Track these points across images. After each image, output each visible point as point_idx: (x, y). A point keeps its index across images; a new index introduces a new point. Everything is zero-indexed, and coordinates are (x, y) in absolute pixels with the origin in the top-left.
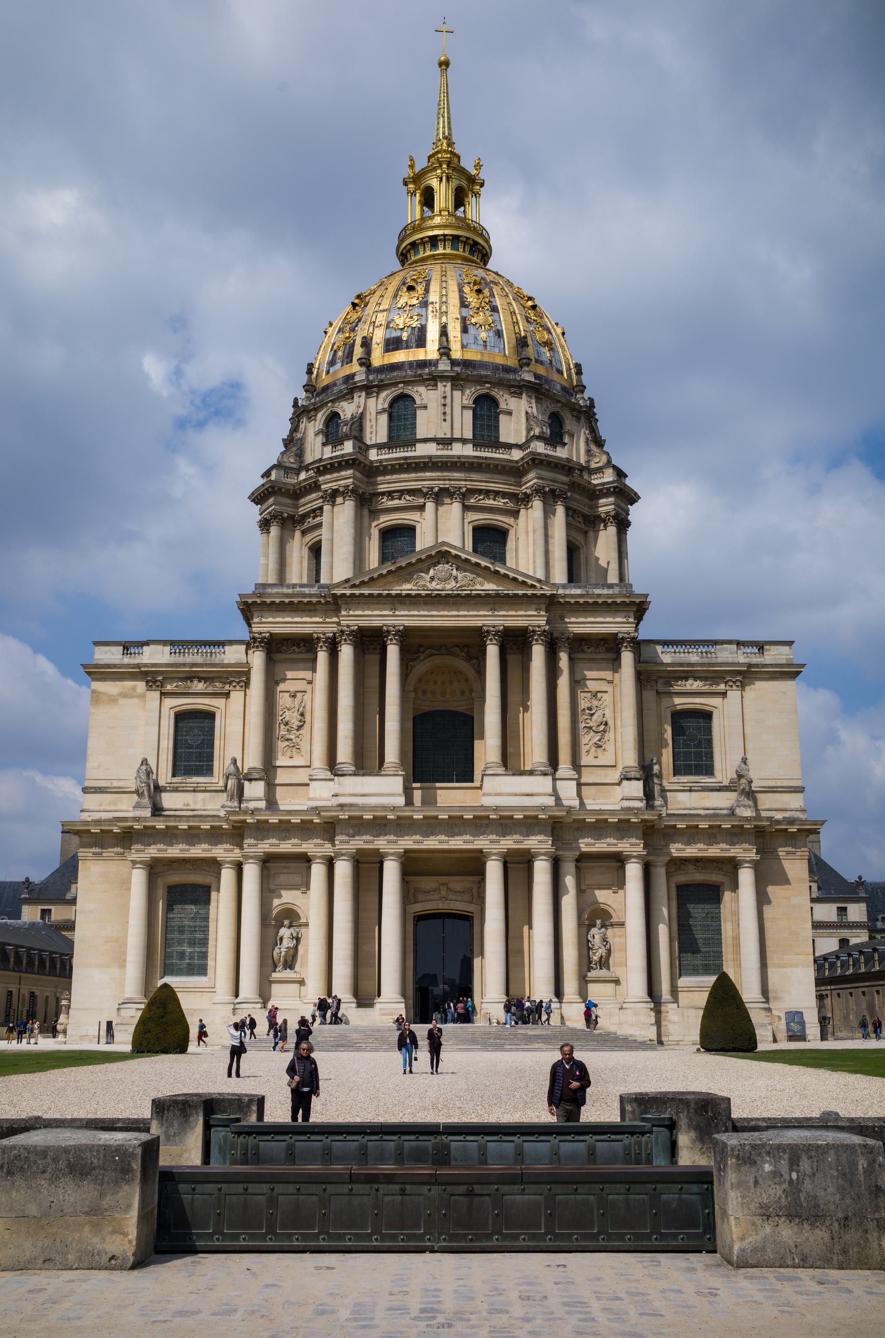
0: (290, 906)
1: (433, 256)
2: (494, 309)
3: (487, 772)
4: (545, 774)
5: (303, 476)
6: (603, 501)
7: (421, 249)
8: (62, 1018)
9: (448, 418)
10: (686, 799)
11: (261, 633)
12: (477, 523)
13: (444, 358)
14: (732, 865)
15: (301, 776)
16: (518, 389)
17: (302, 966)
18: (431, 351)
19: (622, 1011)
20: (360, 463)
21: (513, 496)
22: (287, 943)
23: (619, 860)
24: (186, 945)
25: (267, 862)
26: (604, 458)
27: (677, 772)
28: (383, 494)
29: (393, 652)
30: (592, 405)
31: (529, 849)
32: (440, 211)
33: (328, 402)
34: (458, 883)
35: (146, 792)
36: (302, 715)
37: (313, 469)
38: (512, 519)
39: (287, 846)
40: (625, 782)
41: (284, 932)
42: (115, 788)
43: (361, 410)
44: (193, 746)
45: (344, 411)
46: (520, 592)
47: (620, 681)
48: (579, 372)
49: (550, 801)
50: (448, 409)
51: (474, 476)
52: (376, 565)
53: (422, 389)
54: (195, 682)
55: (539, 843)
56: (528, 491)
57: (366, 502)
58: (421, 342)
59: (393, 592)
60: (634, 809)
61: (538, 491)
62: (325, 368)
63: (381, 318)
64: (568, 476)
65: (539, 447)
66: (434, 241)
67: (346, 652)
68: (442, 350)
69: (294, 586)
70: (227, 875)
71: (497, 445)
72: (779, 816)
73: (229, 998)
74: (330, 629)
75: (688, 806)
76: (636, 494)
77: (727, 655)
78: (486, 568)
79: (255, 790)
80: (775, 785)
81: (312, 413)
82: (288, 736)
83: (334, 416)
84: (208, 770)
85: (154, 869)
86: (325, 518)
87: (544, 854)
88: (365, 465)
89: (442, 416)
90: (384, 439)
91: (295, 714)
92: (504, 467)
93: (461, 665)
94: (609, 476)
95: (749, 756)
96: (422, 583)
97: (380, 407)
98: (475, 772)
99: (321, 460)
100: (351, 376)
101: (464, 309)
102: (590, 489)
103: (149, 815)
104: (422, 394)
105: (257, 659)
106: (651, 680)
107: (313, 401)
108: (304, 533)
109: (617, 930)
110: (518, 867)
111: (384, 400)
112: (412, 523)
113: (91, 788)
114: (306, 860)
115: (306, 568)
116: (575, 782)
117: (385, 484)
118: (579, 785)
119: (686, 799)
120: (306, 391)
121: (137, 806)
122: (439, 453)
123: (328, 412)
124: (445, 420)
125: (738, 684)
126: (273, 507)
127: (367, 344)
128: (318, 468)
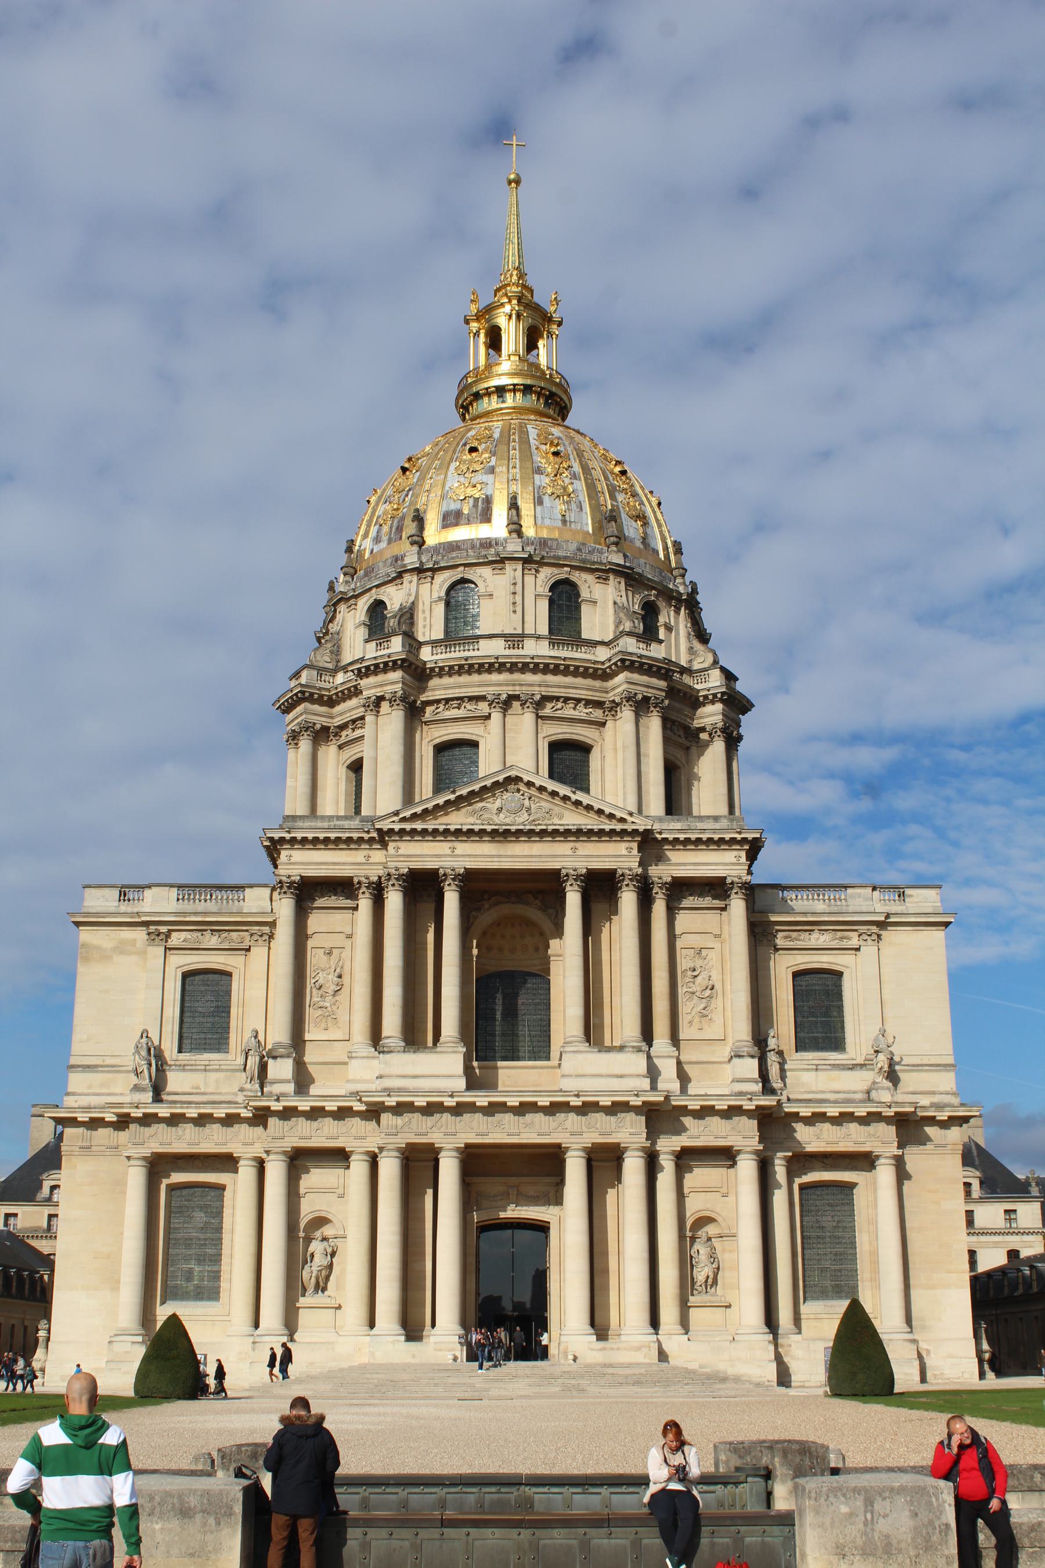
0: (323, 1214)
1: (501, 409)
2: (574, 476)
3: (567, 1049)
4: (639, 1050)
5: (340, 678)
6: (709, 709)
7: (486, 400)
8: (40, 1353)
9: (519, 609)
10: (811, 1080)
11: (289, 877)
12: (554, 738)
13: (514, 535)
16: (602, 573)
17: (337, 1289)
18: (497, 528)
19: (733, 1344)
20: (411, 664)
21: (598, 704)
22: (320, 1261)
23: (726, 1156)
24: (193, 1262)
26: (710, 659)
27: (801, 1045)
28: (438, 701)
29: (451, 900)
30: (695, 591)
31: (619, 1144)
32: (509, 356)
33: (370, 589)
35: (146, 1072)
36: (340, 977)
37: (352, 671)
38: (597, 733)
40: (735, 1060)
41: (316, 1247)
42: (108, 1066)
43: (412, 599)
45: (391, 599)
46: (607, 828)
47: (730, 936)
48: (678, 550)
49: (646, 1083)
50: (518, 599)
51: (550, 678)
52: (430, 795)
53: (486, 571)
54: (208, 934)
56: (618, 700)
58: (486, 516)
59: (452, 828)
60: (746, 1094)
62: (368, 544)
64: (665, 680)
65: (631, 645)
66: (501, 391)
67: (394, 901)
68: (511, 526)
69: (330, 818)
71: (577, 641)
72: (925, 1101)
73: (249, 1329)
74: (374, 873)
75: (814, 1089)
76: (748, 701)
78: (565, 798)
79: (281, 1069)
80: (920, 1062)
81: (352, 601)
82: (322, 1004)
83: (379, 605)
85: (158, 1166)
86: (367, 731)
87: (638, 1150)
88: (417, 667)
90: (440, 635)
91: (330, 977)
92: (586, 669)
93: (533, 913)
94: (715, 681)
95: (887, 1027)
96: (486, 816)
97: (435, 595)
98: (552, 1048)
99: (362, 659)
101: (537, 477)
102: (692, 696)
103: (151, 1100)
105: (285, 908)
107: (353, 586)
108: (340, 747)
109: (728, 1243)
111: (441, 587)
112: (474, 738)
113: (79, 1066)
114: (340, 1156)
115: (343, 792)
116: (675, 1061)
117: (438, 688)
118: (679, 1063)
119: (811, 1080)
120: (345, 574)
121: (137, 1088)
122: (508, 652)
123: (371, 601)
124: (515, 612)
125: (875, 937)
126: (304, 716)
128: (359, 670)
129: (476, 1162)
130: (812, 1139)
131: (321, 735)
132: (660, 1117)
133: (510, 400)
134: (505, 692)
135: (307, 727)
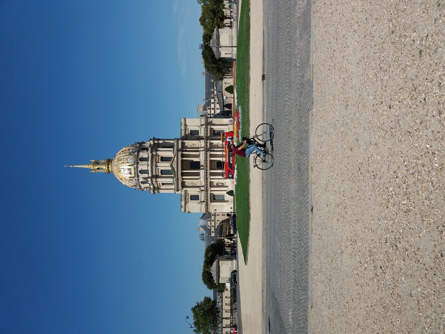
14: (211, 129)
15: (200, 183)
18: (132, 168)
21: (156, 156)
23: (210, 143)
25: (211, 187)
34: (213, 163)
39: (209, 184)
44: (195, 198)
55: (208, 153)
57: (157, 177)
58: (131, 169)
61: (156, 152)
63: (126, 175)
66: (108, 168)
70: (212, 192)
74: (181, 179)
77: (183, 128)
79: (202, 188)
83: (142, 182)
84: (198, 196)
85: (211, 201)
89: (143, 166)
93: (185, 163)
100: (136, 180)
104: (140, 169)
106: (186, 137)
110: (211, 156)
114: (210, 182)
117: (154, 174)
127: (130, 177)
129: (211, 169)
130: (209, 135)
131: (159, 189)
132: (207, 150)
133: (110, 166)
134: (155, 167)
135: (158, 190)
